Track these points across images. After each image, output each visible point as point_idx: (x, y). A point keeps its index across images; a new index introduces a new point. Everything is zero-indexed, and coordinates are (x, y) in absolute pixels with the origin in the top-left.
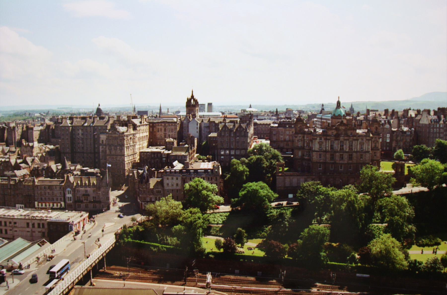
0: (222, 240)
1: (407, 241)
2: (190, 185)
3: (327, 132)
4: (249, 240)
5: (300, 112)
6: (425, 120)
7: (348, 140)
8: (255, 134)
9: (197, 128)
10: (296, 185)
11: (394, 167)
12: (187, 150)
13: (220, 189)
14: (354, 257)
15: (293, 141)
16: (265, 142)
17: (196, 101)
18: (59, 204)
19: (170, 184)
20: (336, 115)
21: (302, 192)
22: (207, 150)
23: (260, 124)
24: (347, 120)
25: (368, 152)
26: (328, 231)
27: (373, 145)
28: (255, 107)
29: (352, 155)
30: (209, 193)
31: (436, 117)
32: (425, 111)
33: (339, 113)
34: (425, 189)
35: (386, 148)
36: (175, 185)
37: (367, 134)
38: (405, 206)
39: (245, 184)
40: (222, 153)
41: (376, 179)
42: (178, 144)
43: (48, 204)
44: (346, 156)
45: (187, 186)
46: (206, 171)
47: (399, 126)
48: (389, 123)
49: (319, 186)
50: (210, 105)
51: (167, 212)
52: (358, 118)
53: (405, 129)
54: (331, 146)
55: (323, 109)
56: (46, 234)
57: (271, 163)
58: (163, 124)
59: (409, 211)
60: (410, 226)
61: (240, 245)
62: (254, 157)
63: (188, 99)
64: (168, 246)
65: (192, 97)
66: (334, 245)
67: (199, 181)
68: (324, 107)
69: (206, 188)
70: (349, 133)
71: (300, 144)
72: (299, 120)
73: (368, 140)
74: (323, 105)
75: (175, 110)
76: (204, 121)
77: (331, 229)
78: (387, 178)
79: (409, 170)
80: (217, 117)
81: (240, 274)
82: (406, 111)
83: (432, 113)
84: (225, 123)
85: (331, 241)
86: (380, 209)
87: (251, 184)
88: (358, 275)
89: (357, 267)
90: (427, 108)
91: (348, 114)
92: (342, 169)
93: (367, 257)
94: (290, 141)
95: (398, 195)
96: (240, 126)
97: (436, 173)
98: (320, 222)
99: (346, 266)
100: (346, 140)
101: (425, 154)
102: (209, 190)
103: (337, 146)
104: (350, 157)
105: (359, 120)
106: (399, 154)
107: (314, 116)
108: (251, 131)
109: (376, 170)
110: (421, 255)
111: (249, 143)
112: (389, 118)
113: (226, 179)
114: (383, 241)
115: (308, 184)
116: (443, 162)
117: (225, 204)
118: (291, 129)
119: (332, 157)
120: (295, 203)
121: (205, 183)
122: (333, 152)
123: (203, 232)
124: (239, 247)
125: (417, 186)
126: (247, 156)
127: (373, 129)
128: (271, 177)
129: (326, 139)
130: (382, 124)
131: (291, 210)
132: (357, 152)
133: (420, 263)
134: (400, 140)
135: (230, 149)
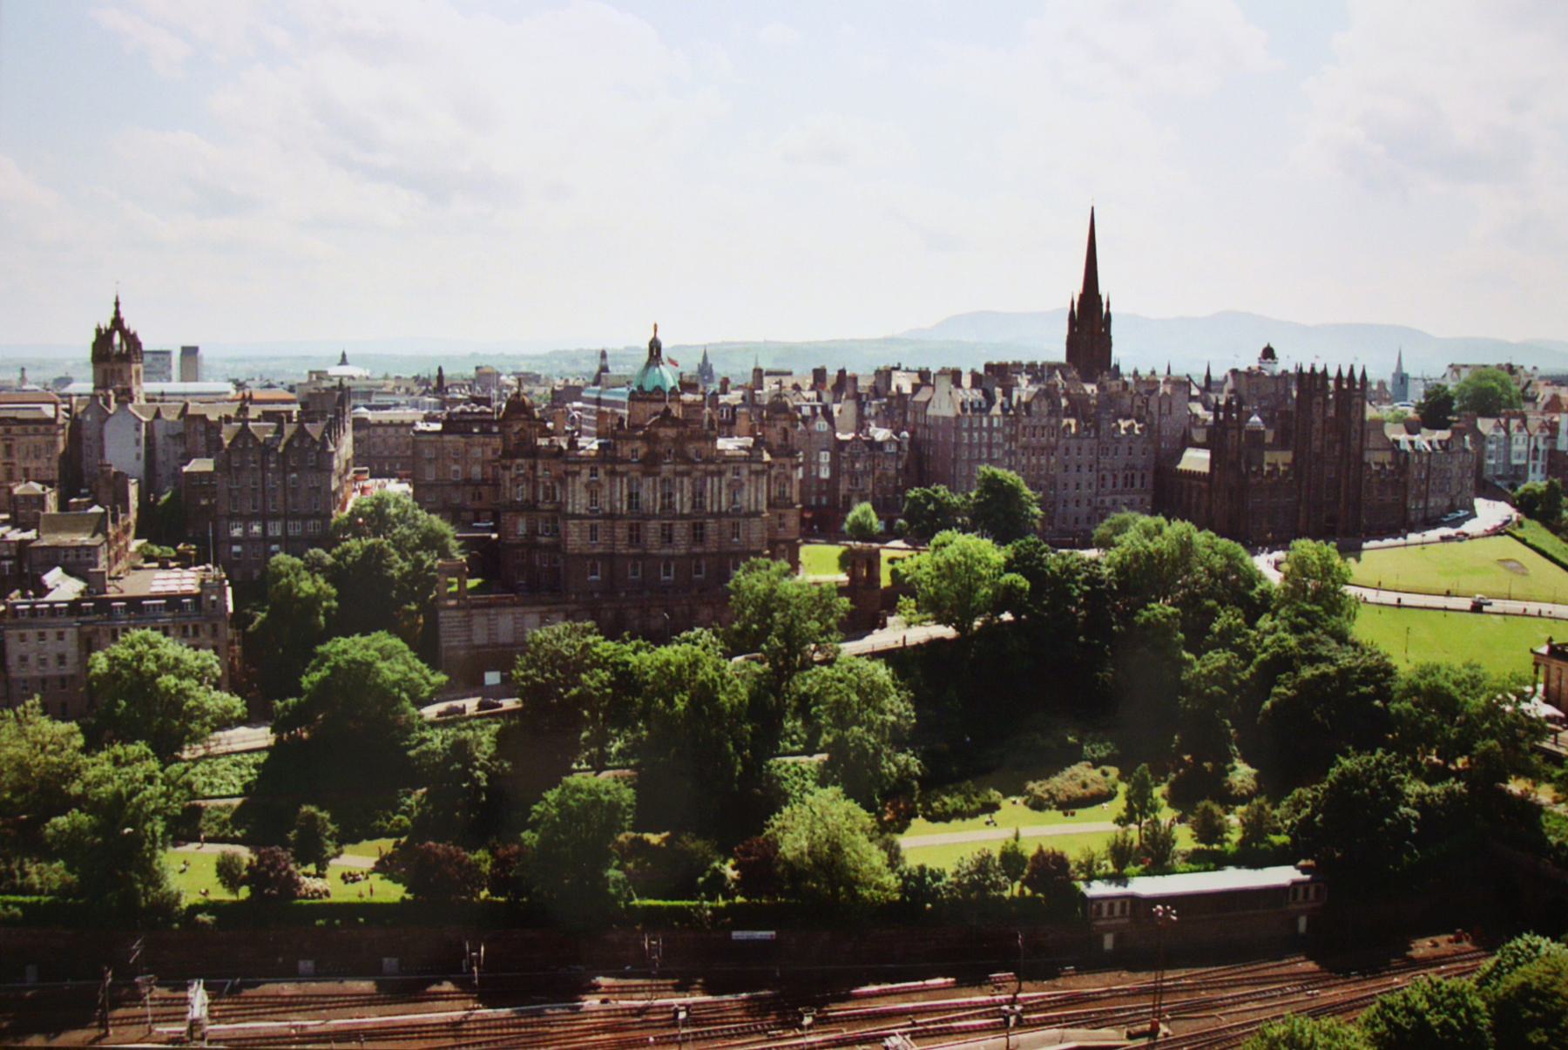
0: (244, 854)
1: (895, 805)
2: (113, 660)
3: (615, 449)
4: (347, 848)
5: (522, 378)
6: (943, 404)
7: (688, 474)
8: (358, 459)
9: (138, 442)
10: (510, 640)
11: (846, 562)
12: (99, 526)
13: (229, 668)
14: (719, 876)
15: (496, 483)
16: (396, 488)
17: (131, 339)
19: (33, 660)
20: (648, 387)
21: (532, 663)
22: (173, 525)
23: (380, 424)
24: (686, 406)
25: (757, 514)
26: (628, 794)
28: (363, 360)
29: (702, 526)
30: (186, 683)
31: (977, 395)
32: (943, 372)
33: (657, 382)
34: (949, 632)
35: (819, 500)
36: (52, 662)
37: (752, 454)
38: (883, 692)
39: (323, 643)
40: (237, 532)
41: (784, 604)
42: (63, 505)
44: (681, 530)
45: (100, 662)
46: (173, 600)
47: (861, 423)
48: (827, 414)
49: (590, 639)
50: (190, 353)
51: (22, 767)
52: (723, 399)
53: (881, 434)
54: (630, 496)
55: (604, 369)
57: (419, 563)
59: (898, 707)
60: (902, 758)
61: (312, 868)
62: (355, 545)
63: (99, 331)
64: (27, 899)
66: (654, 839)
67: (145, 640)
68: (609, 360)
69: (176, 667)
70: (691, 448)
71: (521, 494)
72: (518, 406)
73: (757, 473)
74: (604, 355)
75: (50, 375)
76: (164, 415)
77: (639, 786)
78: (821, 601)
79: (894, 573)
80: (215, 398)
81: (318, 976)
82: (885, 375)
83: (966, 381)
84: (245, 421)
85: (639, 827)
86: (804, 705)
87: (342, 643)
88: (736, 934)
89: (732, 908)
90: (952, 365)
91: (687, 386)
92: (672, 578)
93: (763, 869)
94: (484, 481)
95: (858, 656)
96: (301, 433)
97: (980, 578)
98: (599, 765)
99: (696, 908)
100: (682, 474)
101: (944, 518)
102: (189, 674)
103: (649, 495)
104: (698, 533)
105: (726, 405)
106: (861, 519)
107: (573, 392)
108: (345, 447)
109: (786, 574)
110: (941, 847)
111: (335, 493)
112: (827, 398)
113: (251, 628)
114: (815, 816)
115: (554, 633)
116: (1001, 540)
117: (251, 719)
119: (635, 536)
120: (509, 704)
121: (171, 648)
122: (637, 516)
123: (168, 830)
124: (308, 875)
125: (920, 623)
126: (329, 541)
127: (774, 435)
128: (418, 612)
129: (612, 474)
130: (805, 420)
131: (495, 727)
132: (719, 515)
133: (937, 877)
134: (865, 473)
135: (264, 518)
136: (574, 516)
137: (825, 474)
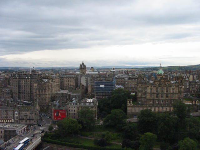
7: (166, 87)
15: (136, 88)
17: (85, 66)
18: (11, 121)
19: (71, 110)
27: (180, 90)
29: (168, 95)
36: (73, 111)
43: (4, 120)
44: (165, 96)
56: (3, 137)
58: (67, 78)
63: (80, 65)
65: (83, 64)
70: (166, 83)
71: (140, 89)
95: (194, 117)
100: (165, 87)
104: (167, 97)
118: (170, 70)
129: (154, 87)
132: (171, 93)
136: (148, 93)
137: (188, 87)
